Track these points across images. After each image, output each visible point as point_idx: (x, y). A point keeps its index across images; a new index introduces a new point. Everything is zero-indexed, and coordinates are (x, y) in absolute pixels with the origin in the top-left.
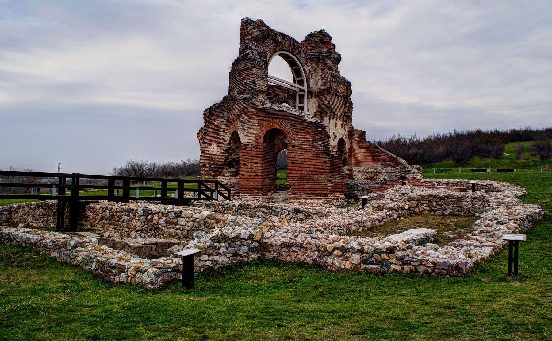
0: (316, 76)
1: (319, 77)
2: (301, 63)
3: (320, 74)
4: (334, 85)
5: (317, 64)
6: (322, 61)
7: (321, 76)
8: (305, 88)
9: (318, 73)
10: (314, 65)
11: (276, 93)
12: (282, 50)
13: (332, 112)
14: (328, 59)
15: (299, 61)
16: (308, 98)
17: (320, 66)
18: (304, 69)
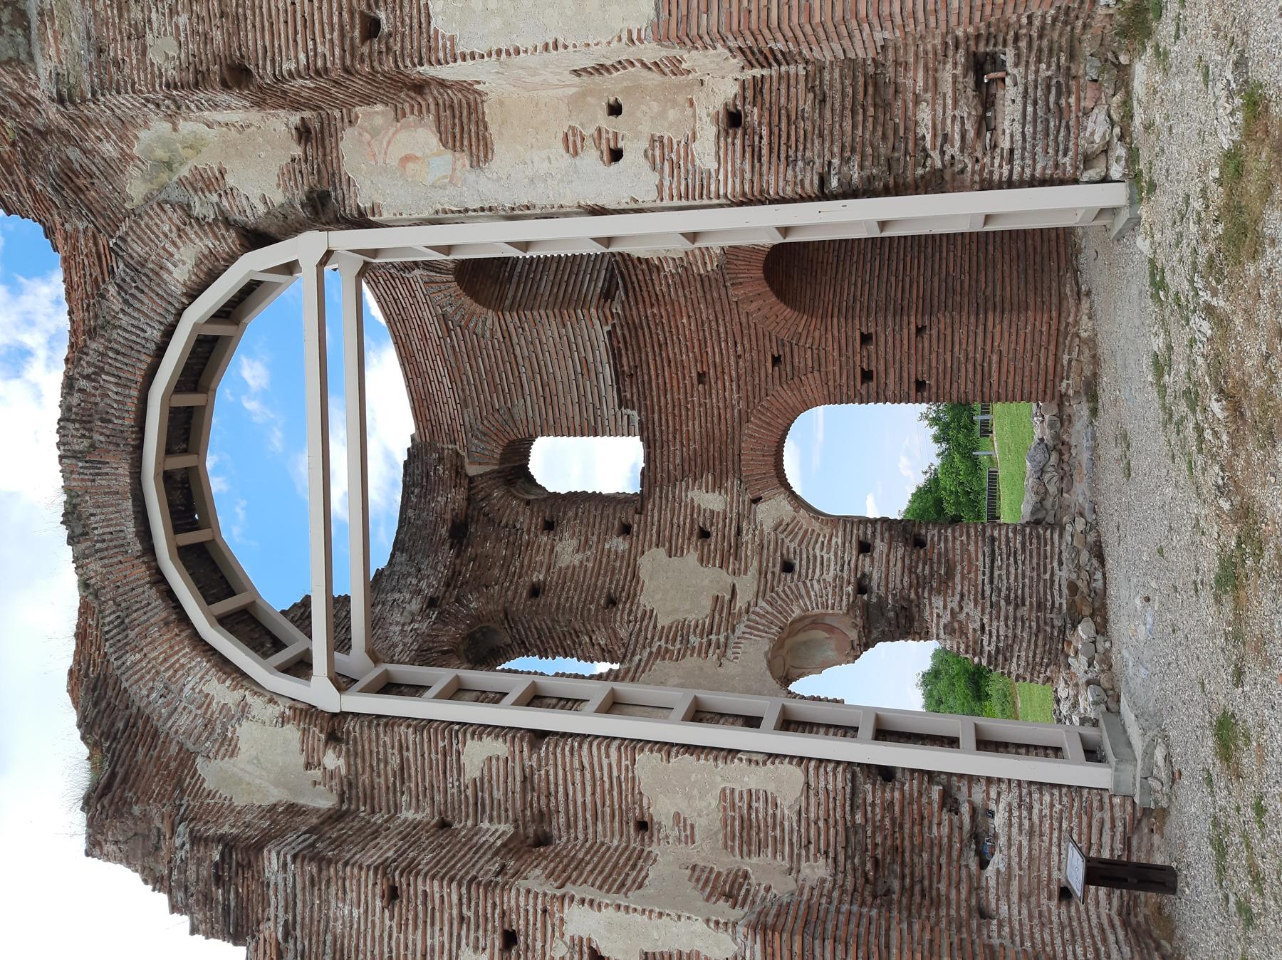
0: (194, 146)
1: (186, 127)
2: (169, 333)
3: (161, 127)
4: (165, 52)
5: (113, 170)
6: (74, 153)
7: (169, 117)
8: (306, 246)
9: (167, 144)
10: (136, 188)
11: (435, 329)
12: (149, 549)
13: (371, 28)
14: (29, 103)
15: (161, 350)
16: (362, 221)
17: (108, 149)
18: (193, 294)
